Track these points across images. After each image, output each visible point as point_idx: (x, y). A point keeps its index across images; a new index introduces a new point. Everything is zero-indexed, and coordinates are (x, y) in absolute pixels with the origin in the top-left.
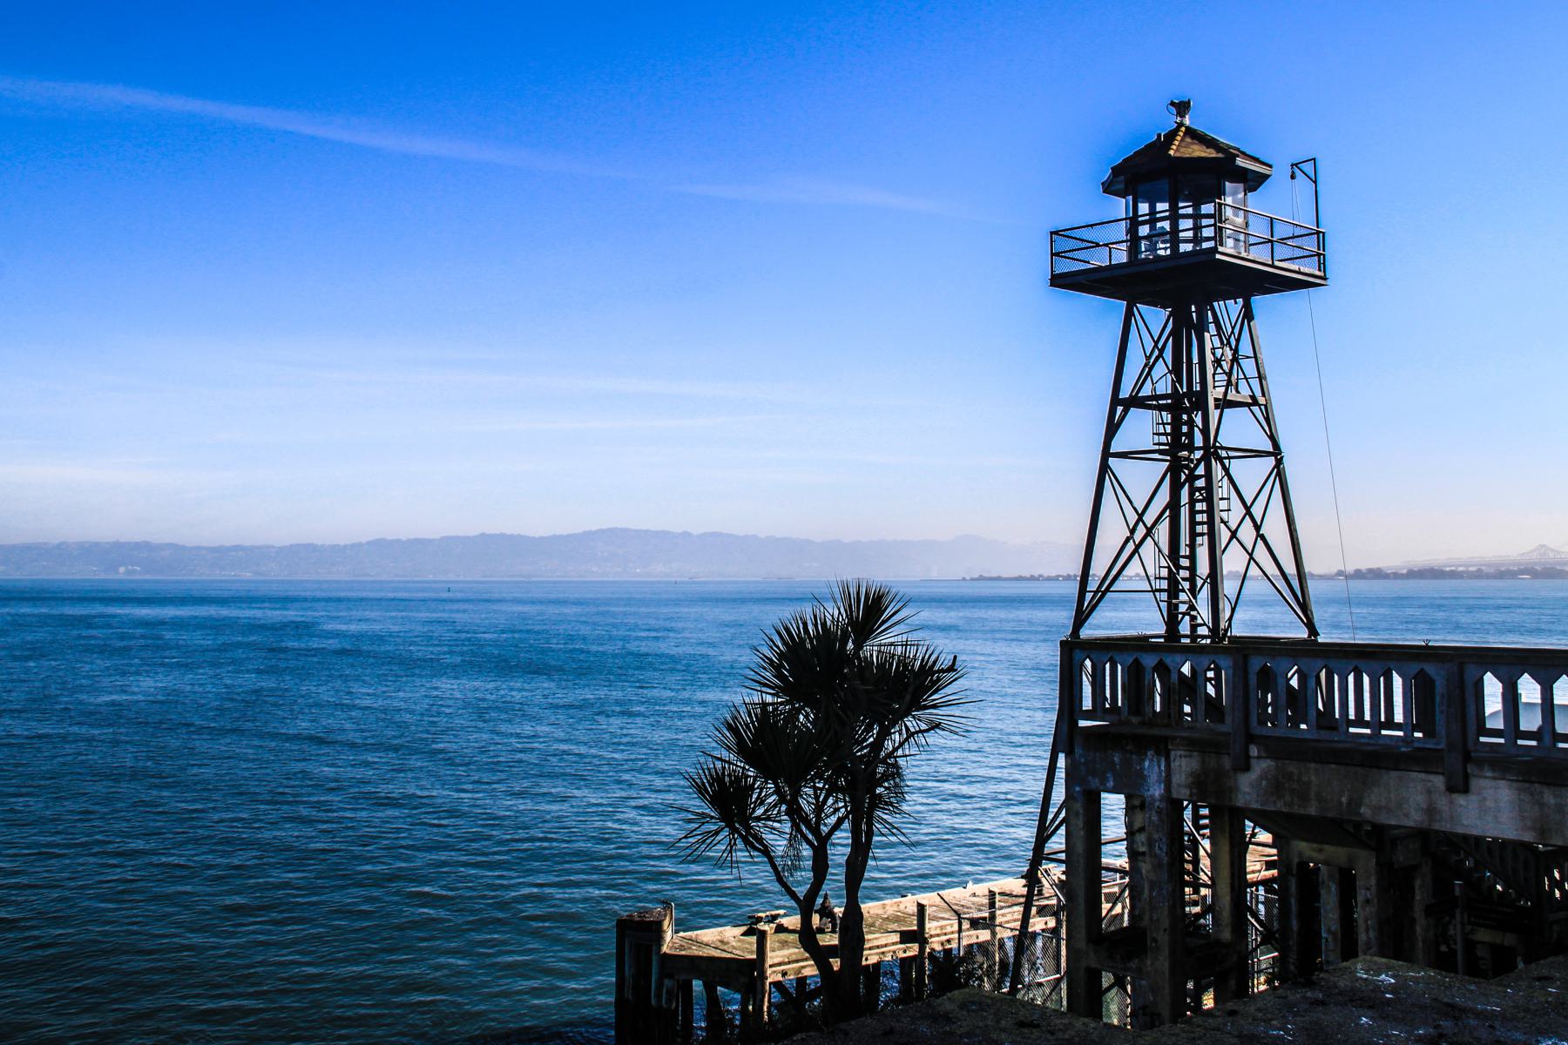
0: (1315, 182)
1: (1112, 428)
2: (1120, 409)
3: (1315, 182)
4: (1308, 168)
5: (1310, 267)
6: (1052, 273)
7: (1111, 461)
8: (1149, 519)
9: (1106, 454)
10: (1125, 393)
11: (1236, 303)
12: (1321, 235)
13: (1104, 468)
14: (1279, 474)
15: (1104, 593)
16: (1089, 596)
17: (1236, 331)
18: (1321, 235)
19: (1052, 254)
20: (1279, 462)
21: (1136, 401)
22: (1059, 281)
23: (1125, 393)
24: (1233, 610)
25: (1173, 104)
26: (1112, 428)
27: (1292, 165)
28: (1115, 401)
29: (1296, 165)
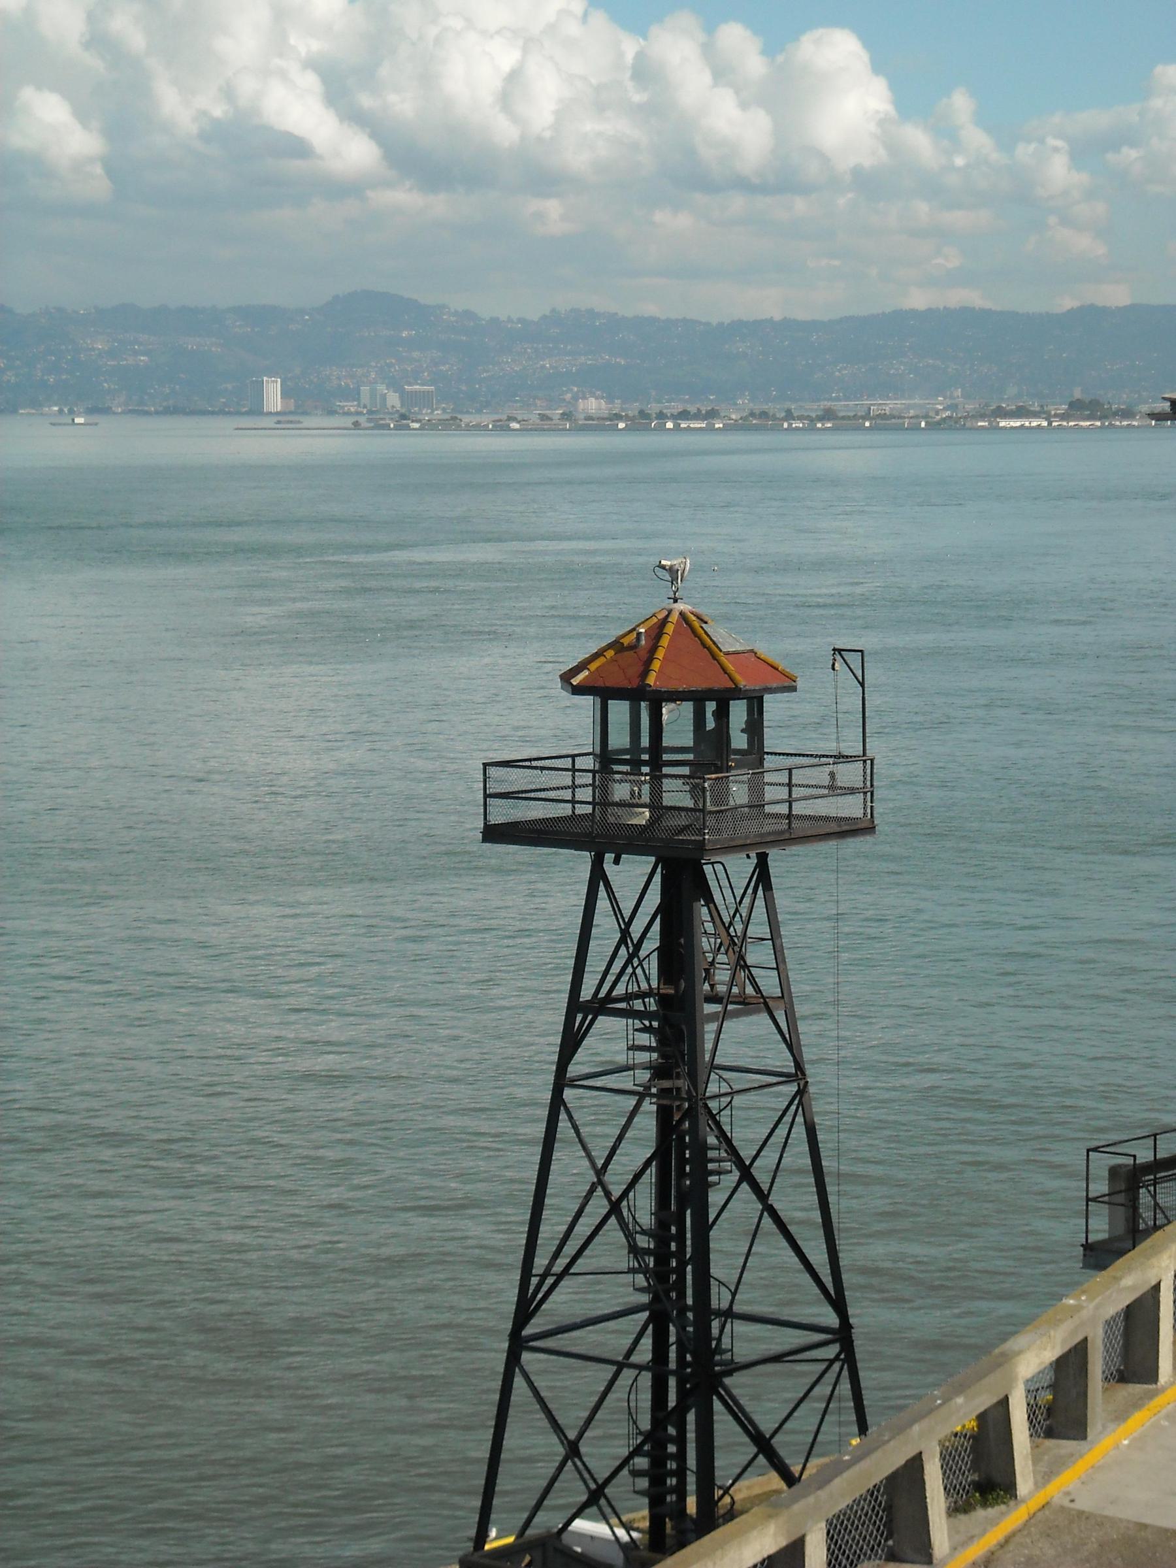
0: (862, 684)
1: (571, 1042)
2: (579, 1017)
3: (862, 684)
4: (854, 660)
5: (851, 807)
6: (485, 823)
7: (568, 1094)
8: (617, 1179)
9: (561, 1081)
10: (586, 994)
11: (748, 857)
12: (869, 762)
13: (557, 1103)
14: (800, 1103)
15: (560, 1277)
16: (534, 1281)
17: (744, 912)
18: (869, 762)
19: (486, 796)
20: (801, 1092)
21: (601, 1006)
22: (494, 833)
23: (586, 994)
24: (734, 1294)
25: (663, 567)
26: (571, 1042)
27: (834, 650)
28: (574, 1005)
29: (840, 651)
